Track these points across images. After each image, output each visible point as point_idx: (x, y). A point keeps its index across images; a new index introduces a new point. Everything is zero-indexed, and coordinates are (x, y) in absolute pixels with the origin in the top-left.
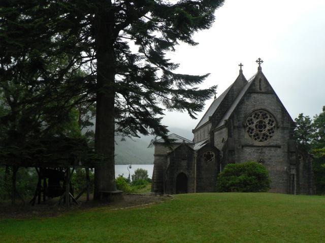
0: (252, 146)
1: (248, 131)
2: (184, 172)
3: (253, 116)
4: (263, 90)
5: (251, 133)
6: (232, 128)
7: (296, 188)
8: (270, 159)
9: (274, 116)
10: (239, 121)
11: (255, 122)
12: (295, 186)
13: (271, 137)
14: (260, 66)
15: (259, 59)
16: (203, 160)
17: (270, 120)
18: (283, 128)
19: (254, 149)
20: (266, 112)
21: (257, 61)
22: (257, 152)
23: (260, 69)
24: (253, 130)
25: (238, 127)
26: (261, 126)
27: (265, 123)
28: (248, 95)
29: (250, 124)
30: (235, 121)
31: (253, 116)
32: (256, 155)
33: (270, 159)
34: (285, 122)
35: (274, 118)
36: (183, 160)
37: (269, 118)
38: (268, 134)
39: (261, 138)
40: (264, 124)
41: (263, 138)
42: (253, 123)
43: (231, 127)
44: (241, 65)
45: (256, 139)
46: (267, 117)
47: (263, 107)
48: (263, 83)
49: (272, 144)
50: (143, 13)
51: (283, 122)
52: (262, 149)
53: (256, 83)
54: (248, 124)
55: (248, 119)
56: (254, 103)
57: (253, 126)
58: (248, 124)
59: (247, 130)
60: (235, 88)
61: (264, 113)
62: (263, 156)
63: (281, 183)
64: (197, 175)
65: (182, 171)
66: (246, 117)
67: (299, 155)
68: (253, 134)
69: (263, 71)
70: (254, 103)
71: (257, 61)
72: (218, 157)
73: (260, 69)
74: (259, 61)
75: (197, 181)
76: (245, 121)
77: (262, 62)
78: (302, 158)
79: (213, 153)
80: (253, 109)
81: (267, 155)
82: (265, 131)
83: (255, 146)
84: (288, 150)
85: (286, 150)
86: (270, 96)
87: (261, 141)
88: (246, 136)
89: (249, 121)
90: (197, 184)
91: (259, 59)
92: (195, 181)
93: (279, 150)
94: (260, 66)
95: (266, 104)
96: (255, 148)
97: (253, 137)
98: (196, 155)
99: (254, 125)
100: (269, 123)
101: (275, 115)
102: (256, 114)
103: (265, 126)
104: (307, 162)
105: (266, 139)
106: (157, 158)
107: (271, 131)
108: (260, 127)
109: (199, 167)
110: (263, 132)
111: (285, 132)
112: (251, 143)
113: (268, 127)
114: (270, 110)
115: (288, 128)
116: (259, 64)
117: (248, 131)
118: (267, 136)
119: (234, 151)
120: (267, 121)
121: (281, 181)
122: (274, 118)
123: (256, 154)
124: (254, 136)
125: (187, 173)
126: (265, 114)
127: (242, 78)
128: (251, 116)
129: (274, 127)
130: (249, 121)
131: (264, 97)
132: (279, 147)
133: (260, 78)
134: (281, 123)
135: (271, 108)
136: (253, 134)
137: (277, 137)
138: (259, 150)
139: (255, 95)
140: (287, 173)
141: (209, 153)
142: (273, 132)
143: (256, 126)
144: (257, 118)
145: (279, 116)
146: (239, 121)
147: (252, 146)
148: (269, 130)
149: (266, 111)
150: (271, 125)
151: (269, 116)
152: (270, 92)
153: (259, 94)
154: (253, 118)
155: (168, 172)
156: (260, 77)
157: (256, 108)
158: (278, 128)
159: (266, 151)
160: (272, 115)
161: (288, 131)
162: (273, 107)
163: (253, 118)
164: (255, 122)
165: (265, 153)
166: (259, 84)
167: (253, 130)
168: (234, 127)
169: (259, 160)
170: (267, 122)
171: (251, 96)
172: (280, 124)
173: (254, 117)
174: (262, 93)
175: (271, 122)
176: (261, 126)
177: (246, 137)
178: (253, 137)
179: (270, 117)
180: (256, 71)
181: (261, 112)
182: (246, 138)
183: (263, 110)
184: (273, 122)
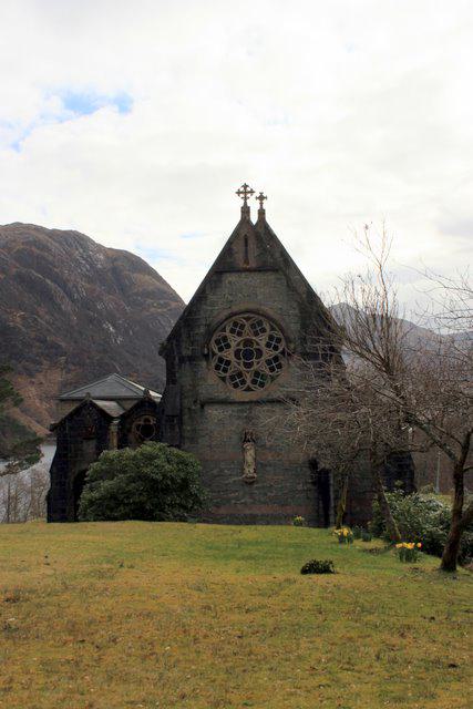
0: (225, 402)
1: (217, 367)
4: (253, 264)
5: (225, 371)
13: (273, 378)
14: (245, 203)
17: (271, 338)
19: (230, 410)
20: (261, 318)
21: (239, 193)
22: (239, 418)
25: (191, 359)
27: (258, 344)
29: (221, 349)
35: (282, 330)
37: (268, 332)
38: (267, 372)
41: (254, 382)
42: (228, 346)
45: (236, 386)
47: (252, 306)
51: (304, 340)
52: (250, 409)
54: (216, 351)
57: (229, 355)
58: (216, 351)
59: (213, 365)
61: (257, 319)
70: (230, 298)
71: (239, 193)
76: (208, 343)
80: (226, 313)
82: (260, 365)
83: (233, 403)
86: (271, 277)
87: (249, 389)
91: (245, 186)
94: (245, 203)
96: (235, 408)
97: (228, 380)
98: (114, 428)
100: (268, 345)
102: (235, 324)
107: (274, 363)
108: (248, 355)
112: (222, 396)
113: (268, 354)
114: (271, 313)
116: (245, 199)
119: (180, 417)
120: (262, 340)
121: (300, 487)
122: (282, 330)
123: (237, 422)
124: (232, 378)
126: (260, 323)
129: (283, 353)
130: (217, 342)
131: (255, 280)
138: (242, 411)
139: (232, 278)
143: (237, 354)
144: (239, 334)
147: (225, 402)
148: (268, 362)
149: (262, 315)
150: (276, 348)
151: (268, 327)
154: (227, 333)
156: (243, 232)
157: (235, 309)
164: (233, 344)
167: (228, 363)
168: (182, 360)
170: (263, 343)
171: (220, 281)
173: (232, 331)
174: (249, 270)
175: (273, 342)
176: (247, 354)
177: (210, 382)
178: (228, 380)
179: (273, 329)
181: (248, 319)
182: (211, 382)
184: (279, 340)
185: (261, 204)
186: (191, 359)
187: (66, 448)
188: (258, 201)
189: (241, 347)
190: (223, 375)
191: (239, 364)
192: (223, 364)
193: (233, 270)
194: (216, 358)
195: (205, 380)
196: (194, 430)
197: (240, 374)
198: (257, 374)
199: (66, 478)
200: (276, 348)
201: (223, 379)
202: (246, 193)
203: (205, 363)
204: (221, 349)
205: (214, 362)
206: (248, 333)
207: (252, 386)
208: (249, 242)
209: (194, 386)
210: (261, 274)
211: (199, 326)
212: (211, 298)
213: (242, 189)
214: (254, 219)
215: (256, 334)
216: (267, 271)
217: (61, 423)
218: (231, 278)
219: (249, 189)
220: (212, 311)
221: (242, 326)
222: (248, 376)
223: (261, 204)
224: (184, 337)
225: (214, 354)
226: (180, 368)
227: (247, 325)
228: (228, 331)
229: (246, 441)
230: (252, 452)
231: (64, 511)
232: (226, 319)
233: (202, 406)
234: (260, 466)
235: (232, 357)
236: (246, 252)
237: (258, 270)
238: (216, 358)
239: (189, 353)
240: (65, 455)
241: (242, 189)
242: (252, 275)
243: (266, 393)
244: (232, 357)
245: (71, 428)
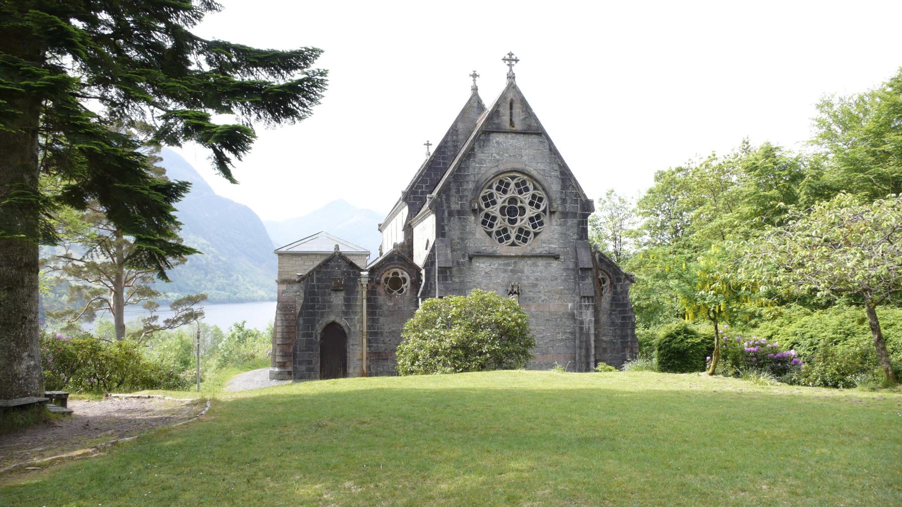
0: (492, 256)
1: (484, 223)
2: (338, 320)
3: (494, 187)
4: (518, 126)
5: (491, 226)
6: (446, 214)
7: (593, 352)
8: (535, 286)
9: (541, 185)
10: (461, 198)
11: (500, 202)
12: (593, 345)
13: (536, 234)
14: (511, 70)
15: (511, 54)
16: (381, 290)
17: (534, 196)
18: (565, 215)
19: (496, 263)
20: (526, 177)
22: (505, 271)
23: (511, 77)
24: (494, 218)
25: (461, 213)
26: (512, 211)
28: (482, 137)
29: (487, 206)
30: (453, 199)
31: (494, 187)
32: (502, 278)
33: (535, 286)
34: (569, 201)
35: (544, 189)
36: (336, 291)
37: (531, 192)
39: (513, 238)
40: (519, 204)
41: (518, 237)
42: (494, 203)
43: (443, 213)
44: (475, 76)
45: (501, 241)
46: (527, 189)
47: (519, 166)
48: (517, 109)
49: (538, 251)
51: (564, 201)
53: (501, 109)
54: (483, 206)
55: (482, 194)
56: (498, 157)
57: (495, 210)
58: (483, 206)
59: (481, 220)
60: (460, 126)
62: (520, 279)
63: (562, 340)
64: (369, 327)
65: (332, 318)
66: (478, 189)
67: (600, 276)
68: (495, 229)
69: (519, 82)
70: (498, 157)
71: (504, 59)
72: (416, 284)
73: (511, 77)
74: (511, 60)
75: (369, 341)
77: (516, 61)
78: (608, 282)
79: (406, 275)
80: (494, 170)
81: (528, 277)
82: (523, 222)
84: (576, 264)
85: (571, 266)
86: (535, 139)
87: (513, 244)
88: (479, 232)
89: (484, 198)
90: (369, 347)
91: (511, 54)
92: (365, 340)
93: (555, 264)
94: (511, 70)
95: (525, 158)
96: (501, 262)
99: (498, 207)
100: (531, 203)
101: (546, 185)
102: (501, 182)
103: (523, 210)
104: (619, 289)
105: (525, 241)
106: (284, 287)
107: (536, 221)
109: (373, 308)
111: (571, 222)
112: (490, 250)
113: (530, 212)
114: (534, 173)
115: (574, 215)
116: (510, 65)
117: (484, 223)
118: (527, 233)
120: (526, 198)
121: (560, 336)
122: (544, 189)
124: (498, 233)
125: (343, 322)
126: (524, 182)
127: (475, 105)
128: (490, 187)
129: (544, 211)
130: (484, 198)
132: (556, 257)
133: (513, 98)
134: (559, 202)
135: (537, 166)
136: (495, 229)
137: (551, 234)
138: (508, 265)
140: (572, 316)
141: (396, 273)
142: (541, 224)
143: (502, 210)
144: (505, 192)
145: (555, 187)
146: (461, 198)
147: (492, 256)
148: (531, 219)
150: (538, 207)
151: (531, 187)
152: (534, 130)
153: (509, 136)
154: (494, 191)
155: (301, 322)
156: (510, 96)
157: (502, 168)
158: (552, 213)
159: (526, 267)
161: (575, 221)
162: (541, 166)
163: (494, 191)
164: (500, 202)
165: (522, 272)
166: (508, 112)
167: (494, 218)
168: (451, 214)
169: (510, 289)
170: (527, 201)
171: (489, 140)
172: (557, 205)
173: (498, 189)
174: (517, 133)
175: (535, 201)
176: (512, 211)
177: (478, 236)
179: (535, 188)
180: (503, 85)
182: (478, 237)
184: (541, 199)
185: (474, 80)
186: (461, 213)
187: (313, 300)
188: (472, 78)
189: (506, 204)
190: (490, 230)
191: (504, 220)
192: (488, 221)
193: (500, 131)
194: (483, 214)
195: (474, 234)
196: (462, 282)
197: (505, 230)
198: (521, 230)
199: (313, 330)
200: (538, 207)
201: (490, 234)
202: (510, 60)
203: (473, 218)
205: (481, 217)
206: (512, 192)
207: (516, 242)
208: (514, 106)
209: (462, 239)
210: (526, 136)
211: (468, 182)
212: (480, 155)
213: (508, 57)
215: (520, 192)
216: (532, 134)
217: (309, 274)
218: (497, 138)
219: (514, 57)
220: (480, 168)
221: (508, 185)
222: (513, 231)
223: (474, 80)
224: (453, 191)
225: (481, 210)
226: (449, 220)
227: (512, 185)
231: (310, 362)
233: (471, 258)
235: (497, 214)
237: (523, 133)
238: (483, 214)
239: (458, 207)
240: (313, 307)
241: (508, 57)
242: (518, 136)
243: (529, 248)
244: (497, 214)
245: (319, 280)
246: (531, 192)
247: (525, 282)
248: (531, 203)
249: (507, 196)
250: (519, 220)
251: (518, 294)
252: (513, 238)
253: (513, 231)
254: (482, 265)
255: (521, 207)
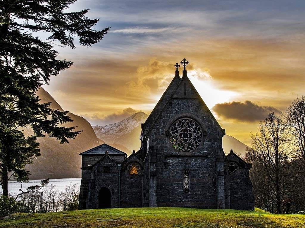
3: (177, 124)
8: (196, 170)
9: (199, 123)
11: (179, 131)
17: (196, 128)
20: (192, 120)
27: (190, 131)
33: (196, 170)
37: (195, 126)
39: (186, 148)
41: (188, 148)
42: (177, 132)
47: (189, 115)
50: (14, 35)
54: (172, 134)
67: (234, 165)
87: (186, 151)
99: (179, 134)
100: (194, 132)
102: (180, 122)
103: (191, 135)
108: (186, 136)
110: (188, 141)
113: (194, 136)
120: (192, 129)
121: (209, 194)
126: (191, 122)
129: (201, 135)
132: (206, 156)
138: (183, 161)
143: (181, 135)
144: (182, 127)
148: (195, 139)
150: (198, 133)
151: (195, 124)
159: (192, 162)
160: (198, 123)
164: (179, 131)
170: (193, 131)
173: (179, 125)
181: (186, 120)
183: (189, 117)
191: (182, 139)
204: (173, 133)
214: (181, 76)
221: (183, 123)
228: (177, 125)
229: (185, 173)
230: (188, 178)
232: (176, 120)
234: (192, 185)
236: (185, 89)
246: (195, 126)
247: (192, 169)
248: (194, 132)
249: (183, 129)
250: (189, 140)
251: (189, 174)
252: (186, 148)
253: (186, 145)
254: (171, 161)
255: (189, 133)
